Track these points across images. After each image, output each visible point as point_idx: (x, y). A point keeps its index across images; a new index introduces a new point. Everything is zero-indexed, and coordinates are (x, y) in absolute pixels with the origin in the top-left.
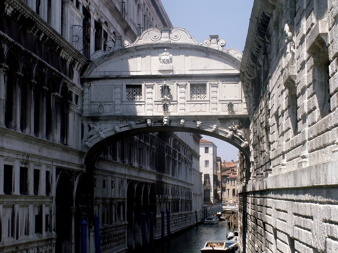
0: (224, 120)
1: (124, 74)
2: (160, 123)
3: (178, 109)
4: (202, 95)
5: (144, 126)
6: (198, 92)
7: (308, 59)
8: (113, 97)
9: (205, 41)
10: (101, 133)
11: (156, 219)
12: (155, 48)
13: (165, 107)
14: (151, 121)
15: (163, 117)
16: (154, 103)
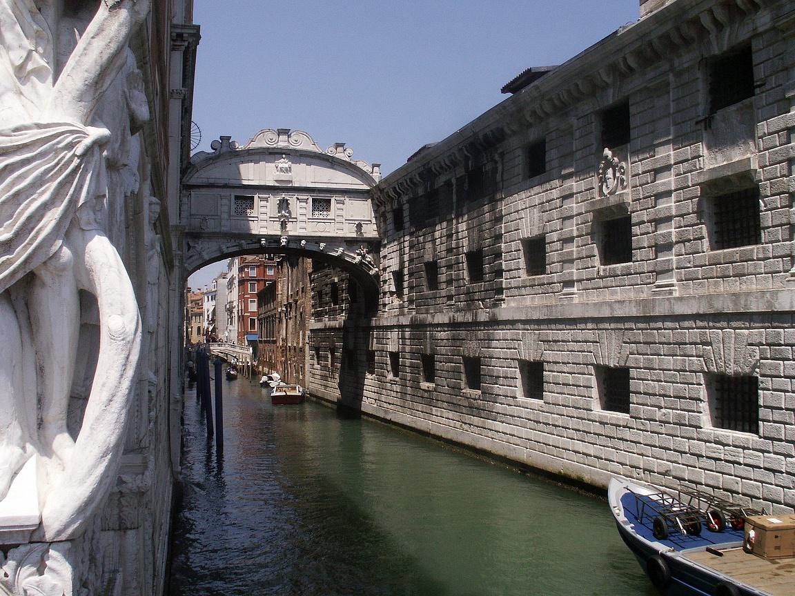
0: (350, 243)
1: (233, 182)
2: (276, 244)
3: (298, 228)
4: (325, 213)
5: (256, 246)
6: (321, 208)
7: (675, 190)
8: (219, 211)
9: (330, 149)
10: (204, 254)
11: (374, 352)
12: (270, 153)
13: (284, 225)
14: (266, 241)
15: (281, 236)
16: (269, 219)
